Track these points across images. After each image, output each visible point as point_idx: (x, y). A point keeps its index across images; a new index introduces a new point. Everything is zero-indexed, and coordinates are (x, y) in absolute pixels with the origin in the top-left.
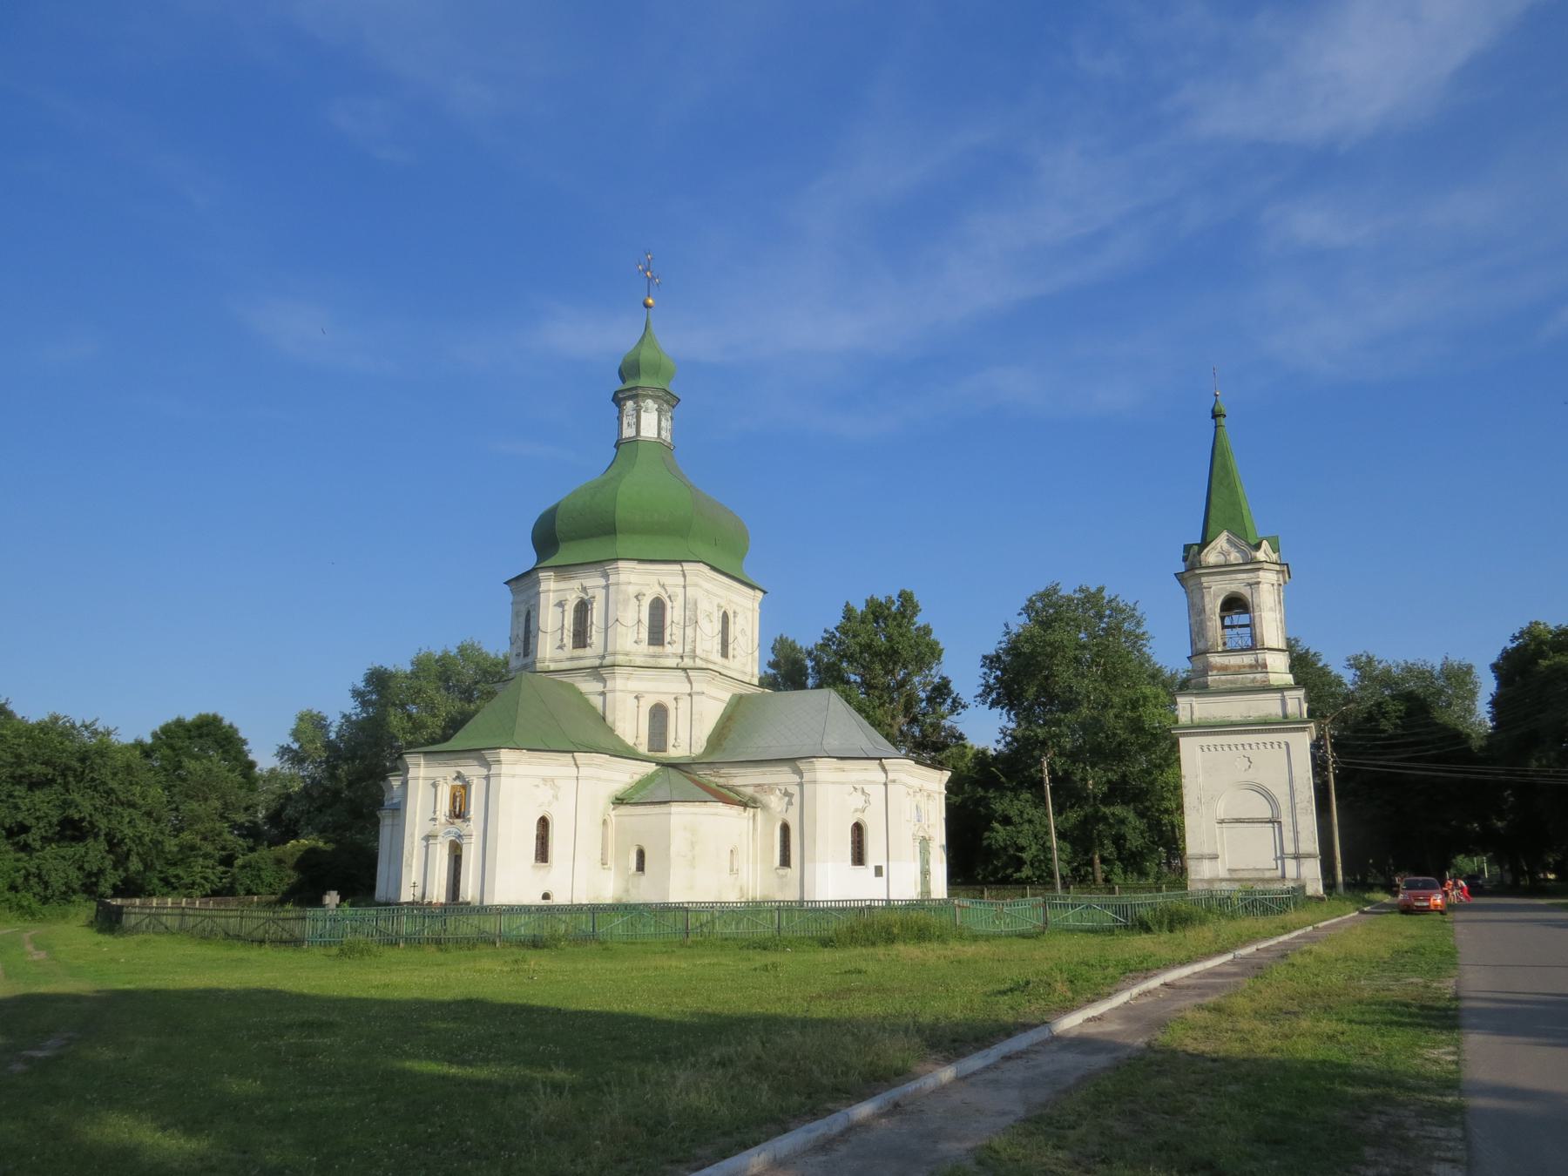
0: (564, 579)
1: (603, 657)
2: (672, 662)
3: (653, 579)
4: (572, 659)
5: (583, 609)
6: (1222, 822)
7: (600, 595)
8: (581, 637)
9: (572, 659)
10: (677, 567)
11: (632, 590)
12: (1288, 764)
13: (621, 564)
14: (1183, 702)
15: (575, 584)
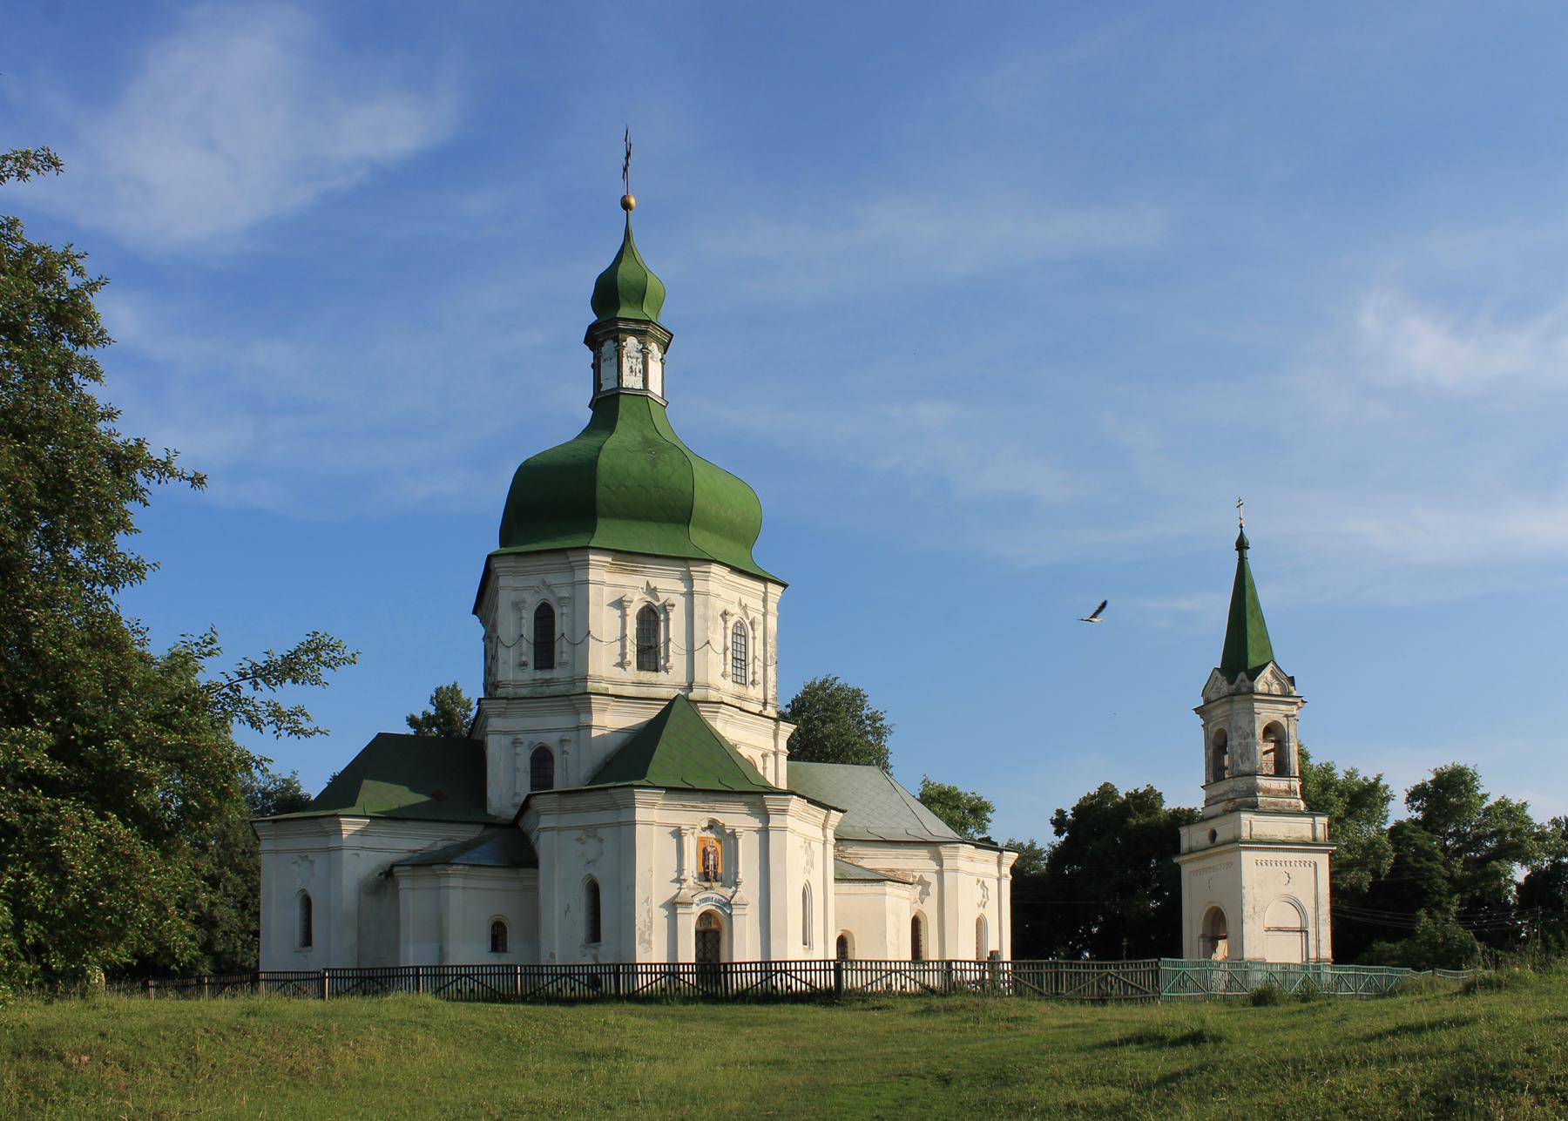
0: (624, 571)
1: (690, 687)
2: (757, 708)
3: (735, 596)
4: (640, 684)
5: (651, 619)
6: (1268, 930)
7: (680, 603)
8: (650, 654)
9: (640, 684)
10: (759, 586)
11: (720, 606)
12: (1310, 880)
13: (714, 568)
14: (1246, 817)
15: (639, 581)
